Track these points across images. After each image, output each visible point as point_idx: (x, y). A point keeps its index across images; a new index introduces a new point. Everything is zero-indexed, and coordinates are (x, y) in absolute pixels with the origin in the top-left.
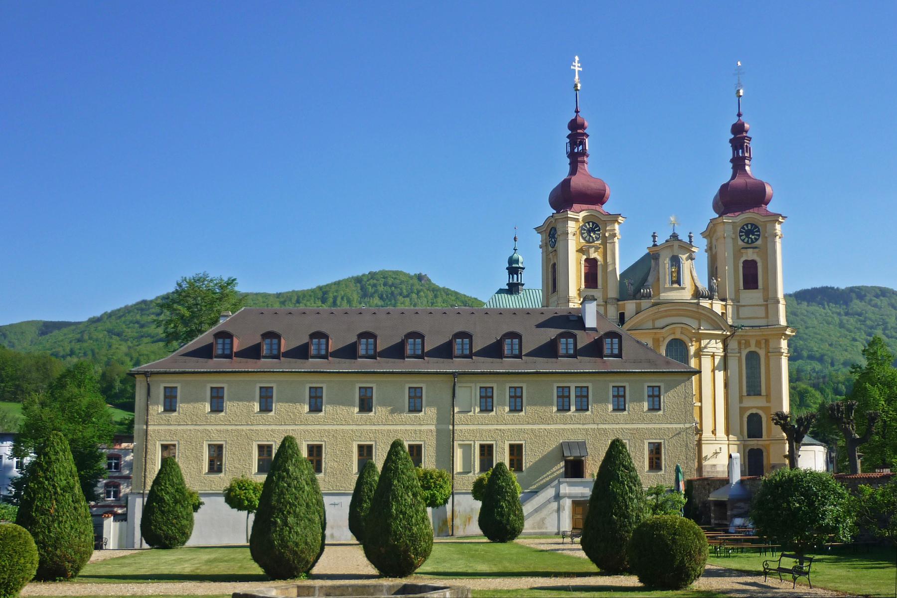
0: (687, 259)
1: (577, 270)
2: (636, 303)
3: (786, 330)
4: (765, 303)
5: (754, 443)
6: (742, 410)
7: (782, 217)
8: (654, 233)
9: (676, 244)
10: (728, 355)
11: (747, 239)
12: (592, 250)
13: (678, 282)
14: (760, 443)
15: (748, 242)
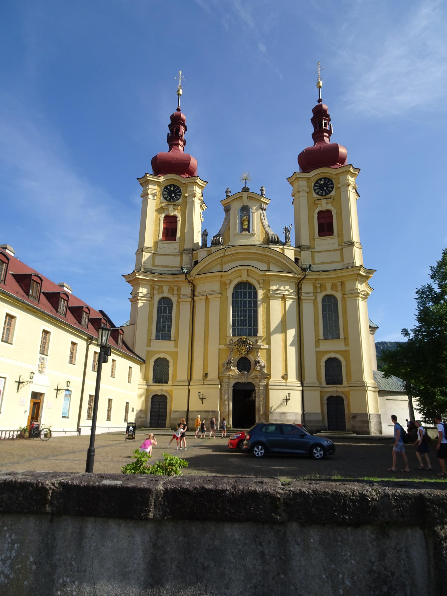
0: (257, 210)
1: (156, 225)
2: (207, 251)
3: (360, 270)
4: (340, 247)
6: (319, 354)
7: (352, 167)
8: (227, 189)
9: (245, 194)
10: (302, 298)
11: (321, 192)
12: (171, 208)
13: (248, 230)
14: (339, 389)
15: (322, 195)
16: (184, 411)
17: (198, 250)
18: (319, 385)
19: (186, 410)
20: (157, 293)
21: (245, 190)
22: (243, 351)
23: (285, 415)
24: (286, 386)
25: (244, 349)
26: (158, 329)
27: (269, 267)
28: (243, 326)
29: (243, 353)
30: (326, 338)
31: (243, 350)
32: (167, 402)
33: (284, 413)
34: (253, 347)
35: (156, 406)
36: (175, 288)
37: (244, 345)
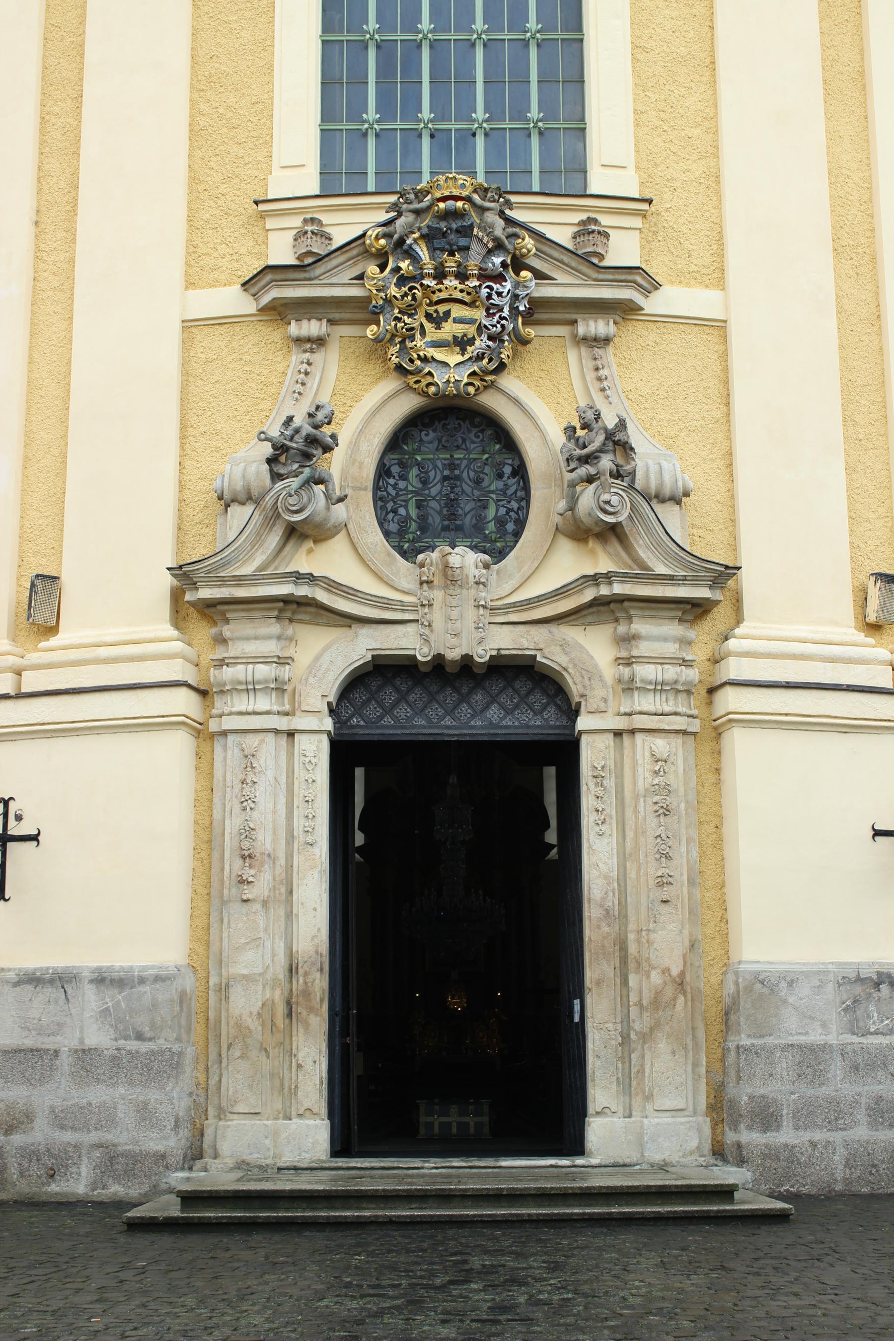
22: (449, 329)
25: (458, 311)
29: (439, 355)
31: (437, 321)
37: (451, 264)
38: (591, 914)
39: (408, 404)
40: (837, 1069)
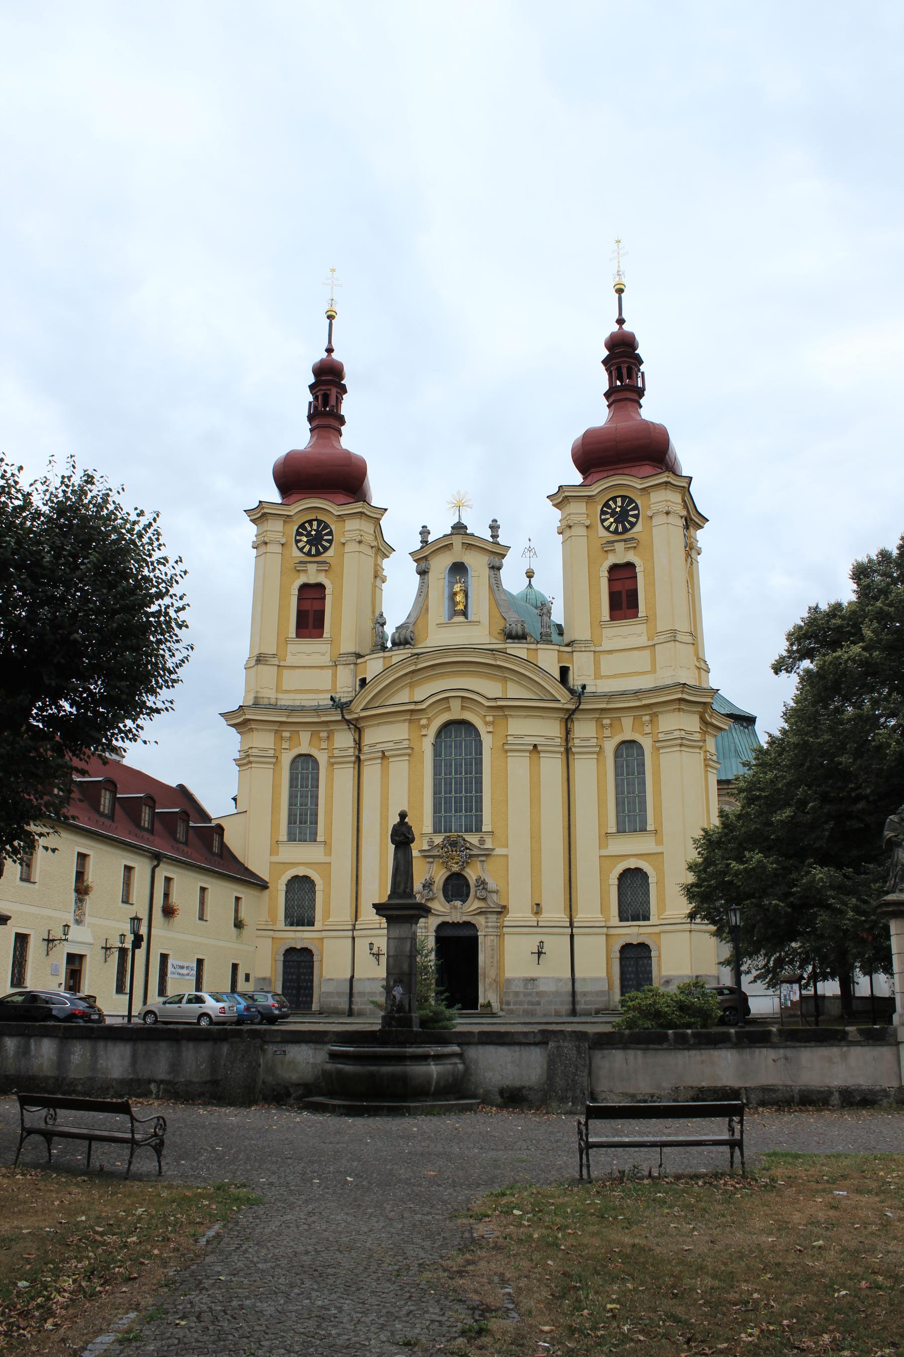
2: (384, 658)
5: (633, 932)
8: (423, 527)
9: (457, 541)
13: (464, 613)
15: (616, 532)
16: (345, 980)
17: (367, 658)
18: (603, 924)
19: (349, 976)
20: (287, 747)
21: (459, 528)
23: (536, 982)
24: (537, 926)
26: (291, 821)
27: (505, 690)
28: (456, 812)
30: (621, 830)
32: (313, 962)
33: (533, 980)
34: (472, 853)
35: (292, 970)
36: (324, 735)
37: (454, 849)
38: (480, 968)
39: (448, 873)
40: (521, 995)
